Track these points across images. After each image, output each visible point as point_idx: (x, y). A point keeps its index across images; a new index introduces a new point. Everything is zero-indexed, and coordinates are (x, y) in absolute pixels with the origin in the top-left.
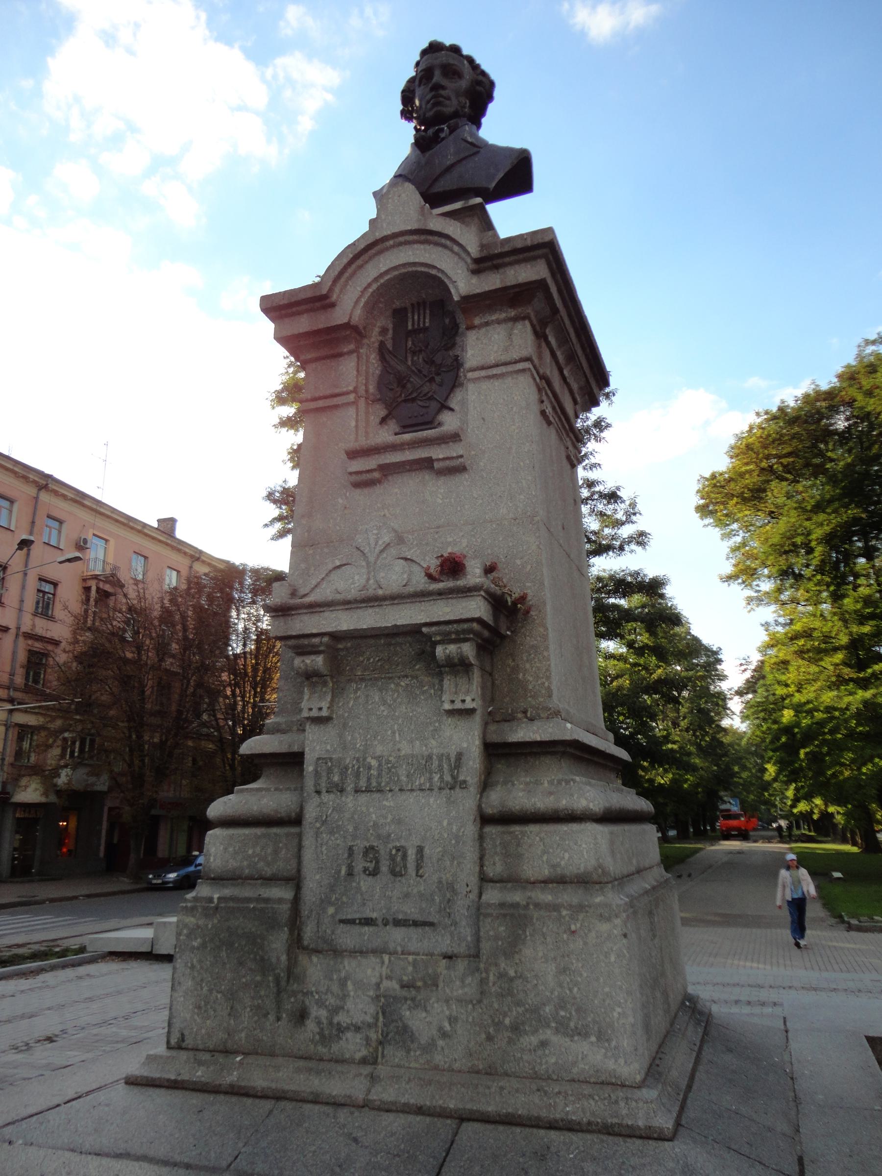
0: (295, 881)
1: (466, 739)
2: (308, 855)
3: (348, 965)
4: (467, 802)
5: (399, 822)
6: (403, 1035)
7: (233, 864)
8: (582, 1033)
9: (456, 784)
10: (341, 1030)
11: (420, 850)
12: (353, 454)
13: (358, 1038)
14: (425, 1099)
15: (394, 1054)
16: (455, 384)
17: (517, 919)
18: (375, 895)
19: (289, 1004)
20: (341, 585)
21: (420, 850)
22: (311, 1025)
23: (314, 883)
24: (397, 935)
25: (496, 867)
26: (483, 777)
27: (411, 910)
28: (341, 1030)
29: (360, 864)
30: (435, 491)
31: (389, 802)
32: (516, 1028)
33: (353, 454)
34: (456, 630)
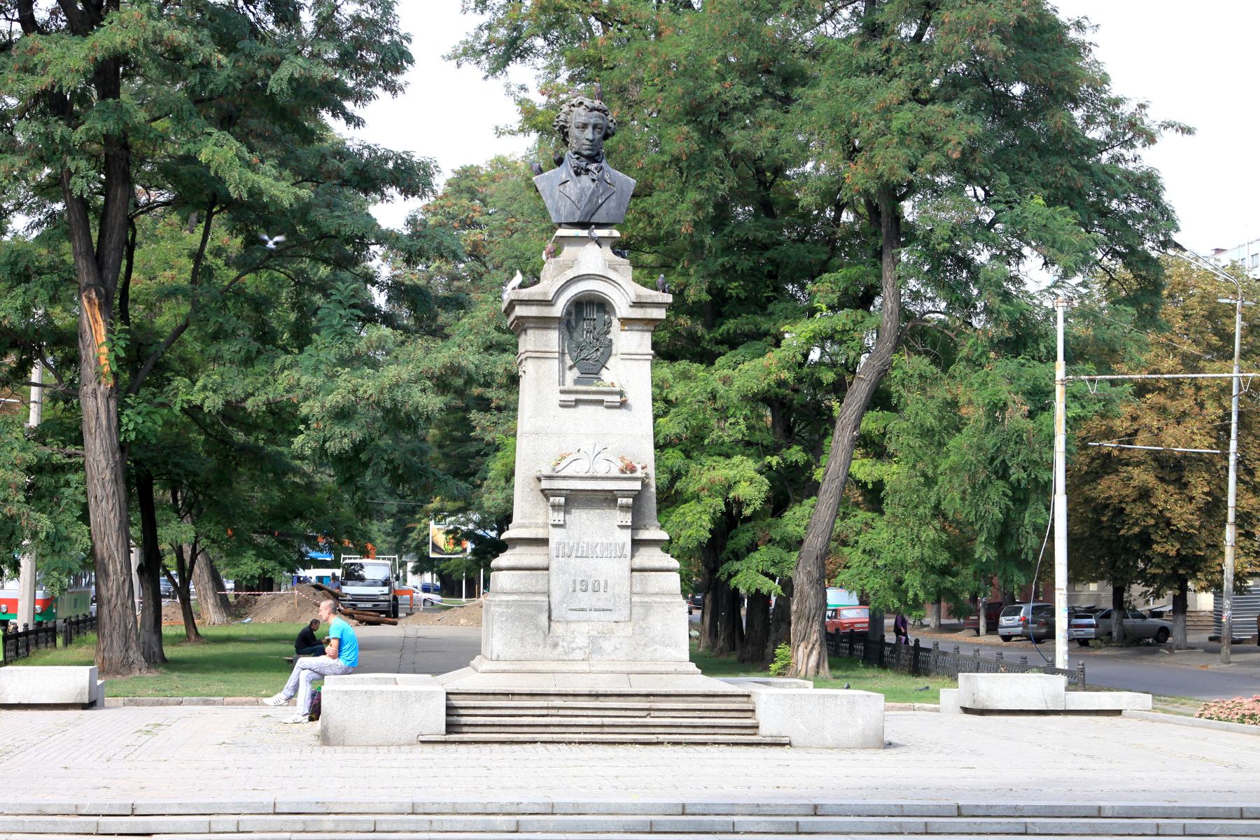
2: (552, 583)
3: (573, 626)
4: (626, 564)
5: (595, 570)
6: (600, 650)
7: (515, 587)
10: (573, 649)
11: (606, 582)
13: (581, 652)
14: (610, 669)
17: (647, 607)
18: (585, 599)
19: (549, 641)
21: (606, 582)
22: (560, 649)
25: (637, 589)
26: (118, 456)
27: (601, 605)
28: (573, 649)
29: (578, 587)
31: (591, 561)
33: (562, 392)
34: (625, 493)
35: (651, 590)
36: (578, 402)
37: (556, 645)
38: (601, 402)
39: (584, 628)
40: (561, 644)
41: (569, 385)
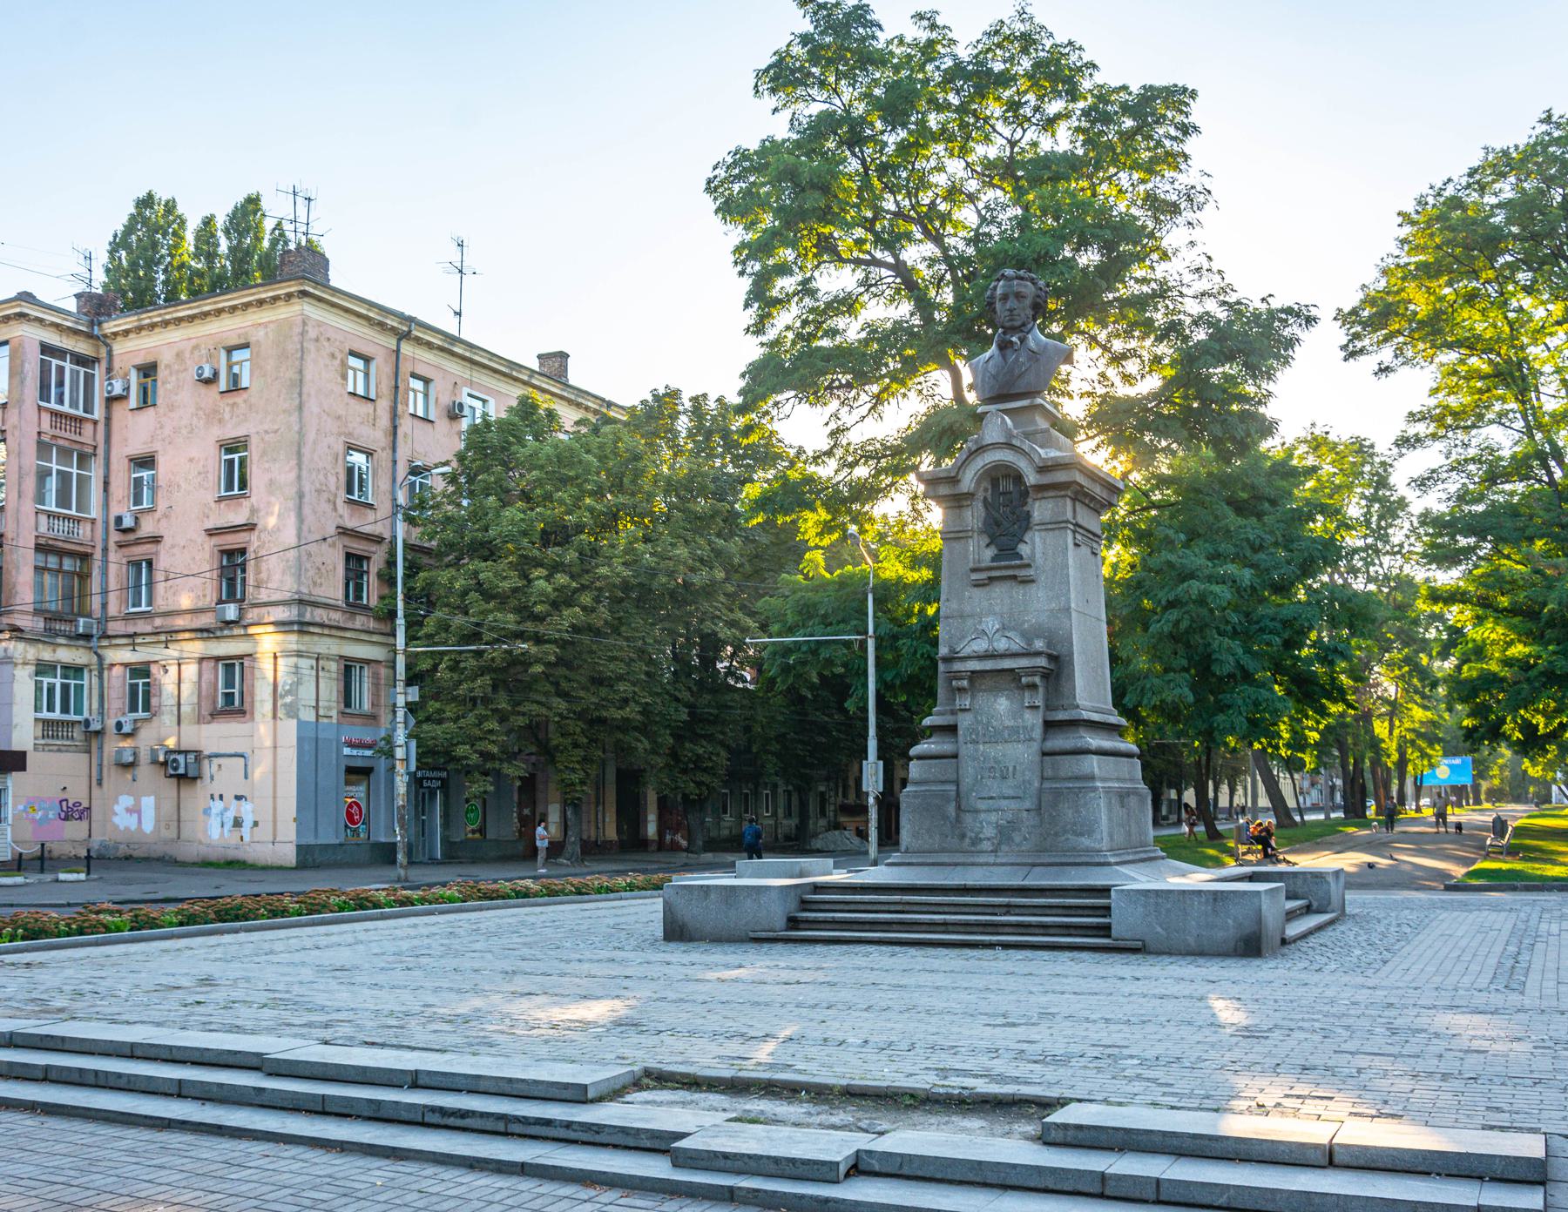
0: (957, 783)
1: (1034, 720)
3: (983, 816)
4: (1035, 746)
8: (1082, 834)
9: (1032, 739)
12: (974, 570)
15: (1004, 848)
16: (1027, 528)
20: (976, 648)
22: (967, 840)
23: (967, 781)
24: (1004, 803)
25: (1049, 773)
27: (1011, 792)
30: (1019, 592)
32: (1056, 834)
33: (974, 570)
34: (1032, 671)
35: (1062, 774)
36: (990, 578)
37: (963, 836)
38: (1014, 577)
39: (993, 817)
40: (969, 834)
41: (987, 563)
